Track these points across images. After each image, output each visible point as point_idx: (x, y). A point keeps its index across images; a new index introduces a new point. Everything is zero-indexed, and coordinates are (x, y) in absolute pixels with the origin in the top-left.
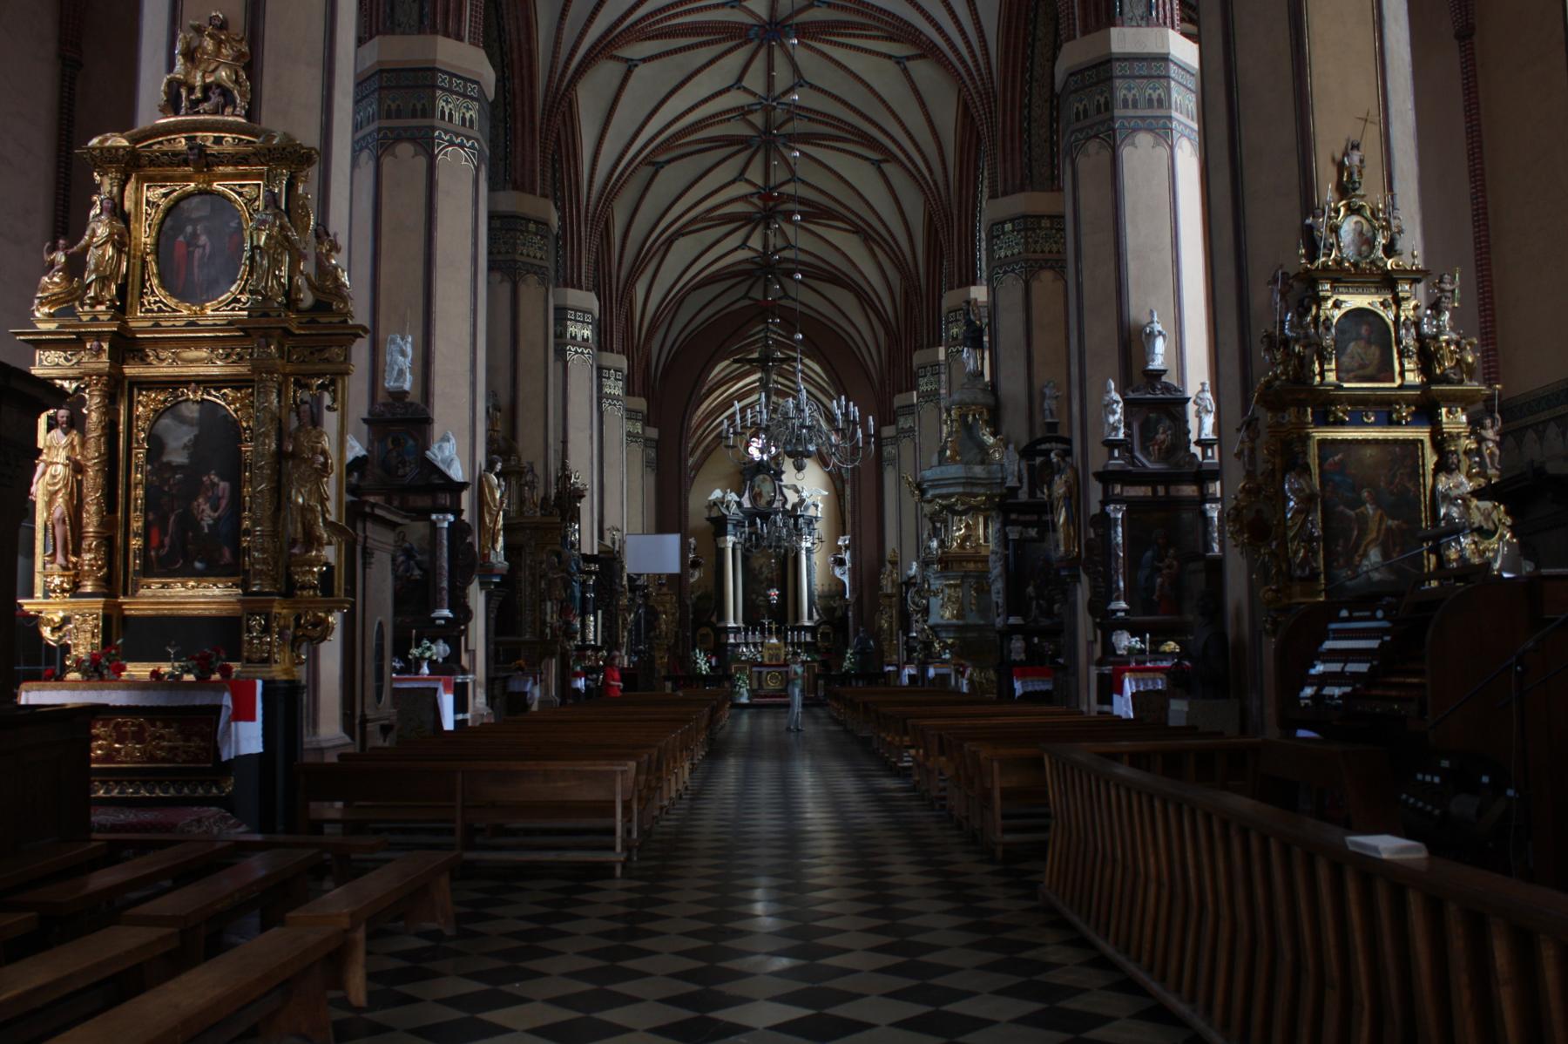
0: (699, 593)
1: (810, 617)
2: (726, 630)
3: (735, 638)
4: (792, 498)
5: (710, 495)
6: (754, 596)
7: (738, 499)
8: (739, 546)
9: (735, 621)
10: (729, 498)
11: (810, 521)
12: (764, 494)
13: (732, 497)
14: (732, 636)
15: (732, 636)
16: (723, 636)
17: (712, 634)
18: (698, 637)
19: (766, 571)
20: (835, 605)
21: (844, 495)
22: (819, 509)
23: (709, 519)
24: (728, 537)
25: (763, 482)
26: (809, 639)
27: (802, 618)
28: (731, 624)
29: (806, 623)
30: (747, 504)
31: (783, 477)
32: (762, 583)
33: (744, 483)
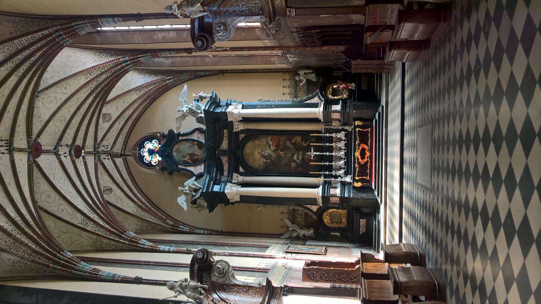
0: (288, 223)
1: (316, 105)
2: (326, 198)
3: (336, 188)
4: (190, 124)
5: (182, 209)
6: (293, 165)
7: (194, 178)
8: (241, 179)
9: (315, 186)
10: (187, 188)
11: (215, 102)
12: (191, 152)
13: (191, 182)
14: (332, 191)
15: (332, 191)
16: (333, 200)
17: (330, 211)
18: (334, 225)
19: (268, 152)
20: (305, 81)
21: (195, 71)
22: (204, 95)
23: (211, 208)
24: (226, 191)
25: (180, 152)
26: (338, 107)
27: (315, 113)
28: (318, 192)
29: (321, 109)
30: (200, 169)
31: (175, 131)
32: (279, 156)
33: (179, 170)
